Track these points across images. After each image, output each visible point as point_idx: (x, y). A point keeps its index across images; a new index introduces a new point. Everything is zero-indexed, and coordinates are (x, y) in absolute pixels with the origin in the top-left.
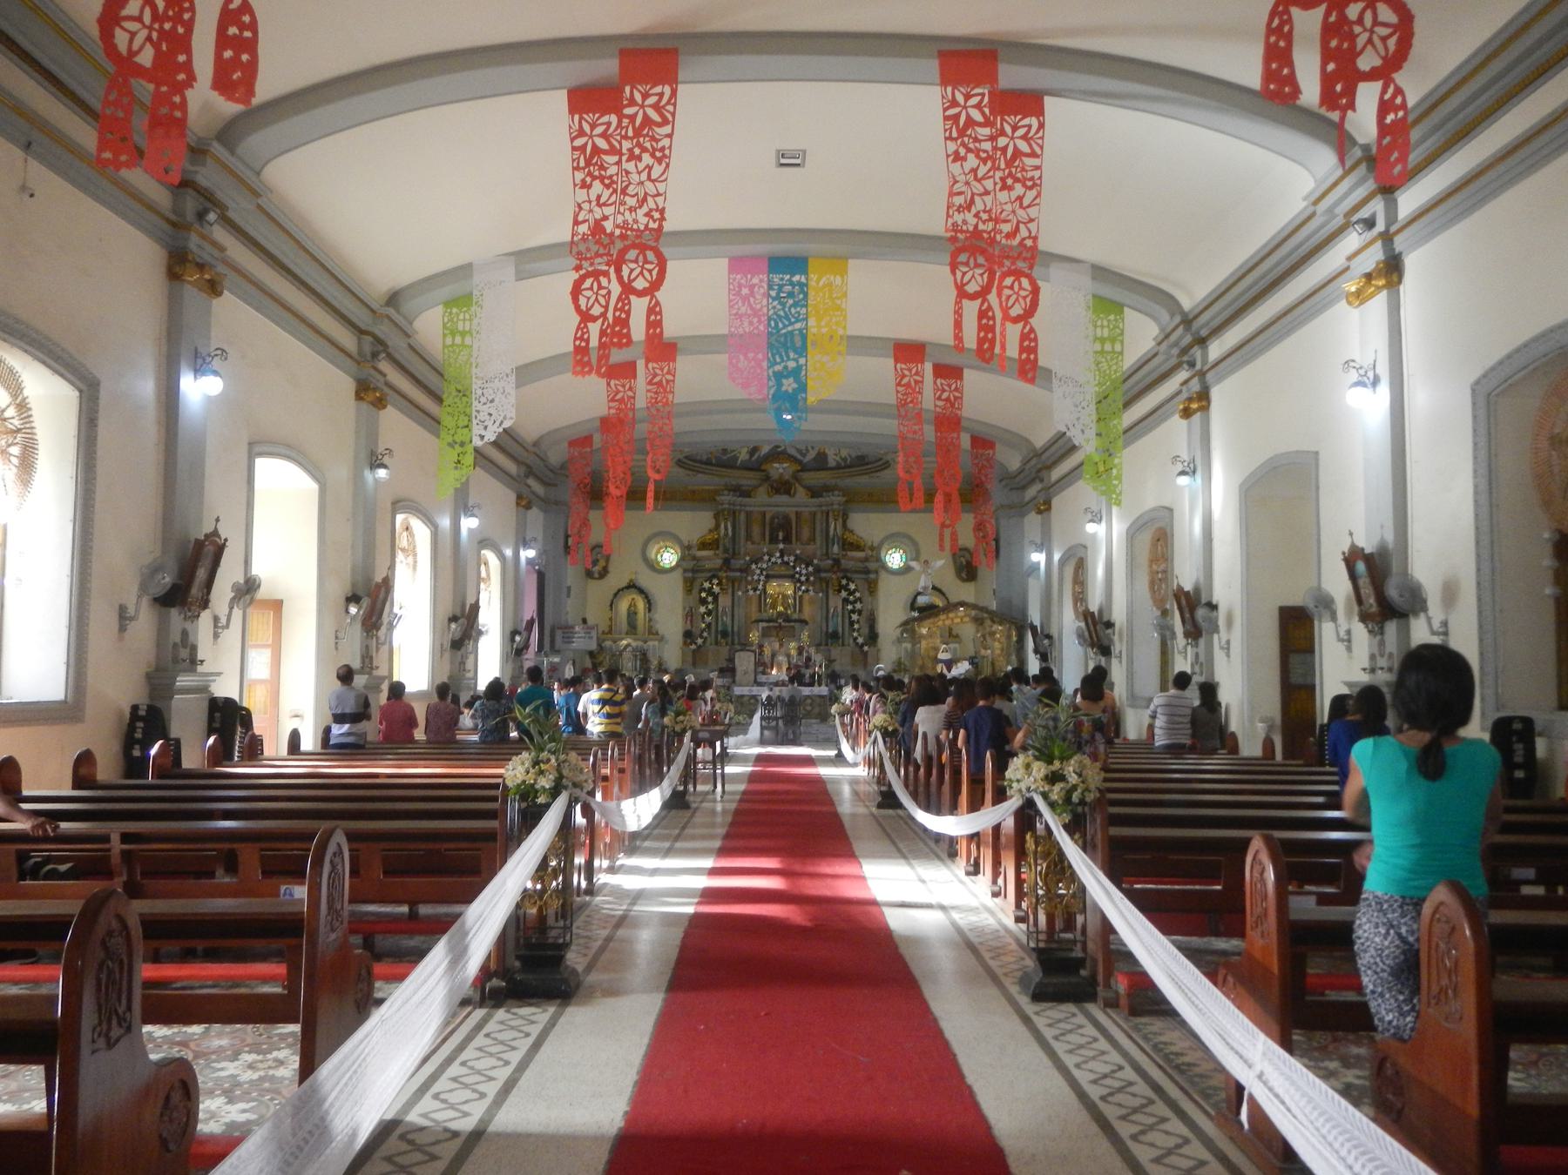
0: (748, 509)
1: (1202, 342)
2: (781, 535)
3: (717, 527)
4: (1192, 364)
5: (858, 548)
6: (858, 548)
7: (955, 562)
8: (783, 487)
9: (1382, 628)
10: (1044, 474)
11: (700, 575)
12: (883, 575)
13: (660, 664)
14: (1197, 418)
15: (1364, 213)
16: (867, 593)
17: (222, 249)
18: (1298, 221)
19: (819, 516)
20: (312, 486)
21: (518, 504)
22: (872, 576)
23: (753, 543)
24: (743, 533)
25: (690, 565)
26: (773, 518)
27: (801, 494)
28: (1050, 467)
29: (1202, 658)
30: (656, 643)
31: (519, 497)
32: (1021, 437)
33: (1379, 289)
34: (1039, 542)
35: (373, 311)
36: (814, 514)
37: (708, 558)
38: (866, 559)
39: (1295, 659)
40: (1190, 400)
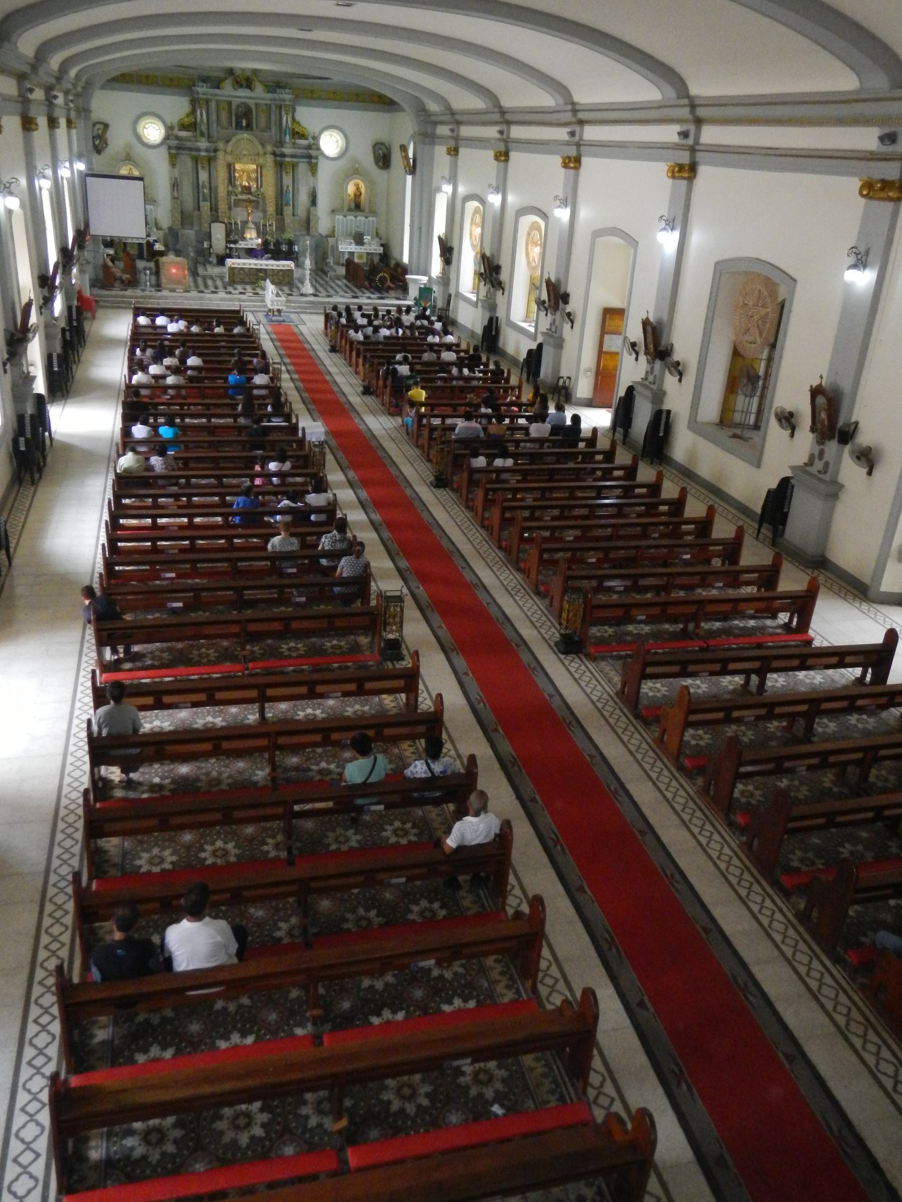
0: (219, 98)
2: (244, 123)
3: (193, 111)
5: (303, 136)
6: (303, 136)
7: (374, 152)
11: (181, 152)
12: (320, 158)
16: (310, 174)
19: (273, 108)
22: (314, 161)
23: (223, 128)
24: (214, 117)
25: (174, 143)
26: (238, 107)
27: (259, 90)
29: (557, 323)
30: (152, 207)
33: (684, 178)
34: (447, 176)
36: (269, 107)
37: (188, 139)
38: (309, 147)
39: (607, 337)
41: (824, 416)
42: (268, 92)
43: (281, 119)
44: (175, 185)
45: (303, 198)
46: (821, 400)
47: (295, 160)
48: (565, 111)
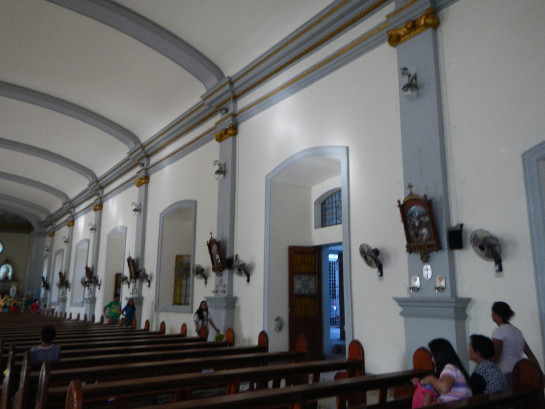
1: (102, 188)
4: (98, 194)
9: (135, 282)
10: (54, 223)
14: (98, 211)
15: (142, 161)
33: (143, 183)
39: (118, 290)
40: (96, 206)
41: (217, 257)
46: (214, 248)
48: (93, 183)
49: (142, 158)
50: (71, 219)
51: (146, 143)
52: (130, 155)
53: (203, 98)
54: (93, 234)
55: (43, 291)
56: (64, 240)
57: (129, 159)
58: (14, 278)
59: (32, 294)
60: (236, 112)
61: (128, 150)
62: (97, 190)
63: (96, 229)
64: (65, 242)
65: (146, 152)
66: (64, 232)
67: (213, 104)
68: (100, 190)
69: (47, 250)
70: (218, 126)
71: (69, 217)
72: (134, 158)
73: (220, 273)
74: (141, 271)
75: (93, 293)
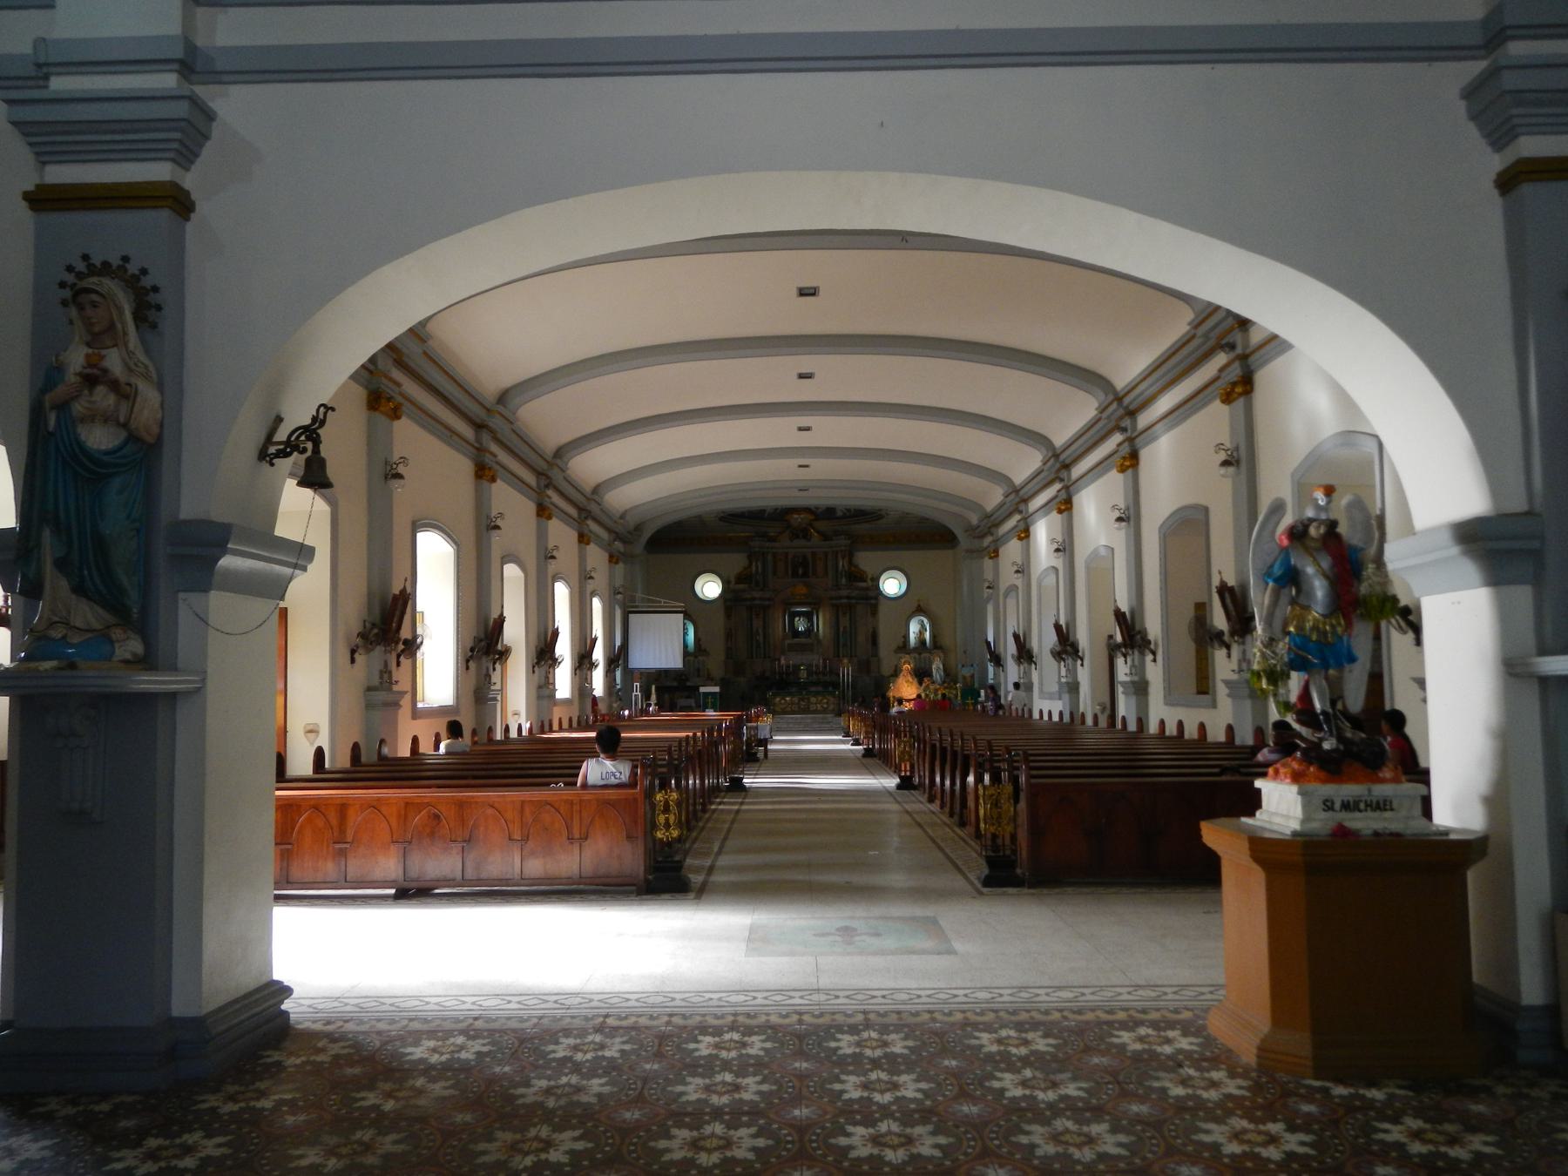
1: (1067, 466)
2: (800, 571)
8: (801, 533)
10: (993, 530)
13: (709, 675)
14: (1065, 514)
17: (495, 456)
18: (1133, 384)
20: (523, 575)
21: (610, 561)
22: (873, 602)
28: (998, 524)
31: (611, 556)
32: (976, 503)
33: (1128, 467)
35: (548, 462)
42: (825, 540)
43: (837, 564)
44: (729, 635)
45: (861, 638)
47: (853, 601)
49: (1121, 418)
50: (1022, 526)
51: (1126, 390)
52: (1102, 411)
53: (1195, 323)
54: (1061, 560)
55: (991, 669)
56: (1015, 568)
57: (1099, 420)
58: (937, 644)
59: (972, 676)
60: (1248, 351)
61: (1096, 405)
62: (1058, 471)
63: (1065, 548)
64: (1017, 572)
65: (1127, 407)
66: (1011, 551)
67: (1212, 335)
68: (1063, 471)
69: (989, 587)
70: (1224, 374)
71: (1018, 521)
72: (1108, 417)
73: (1241, 640)
74: (1139, 632)
75: (1072, 672)
